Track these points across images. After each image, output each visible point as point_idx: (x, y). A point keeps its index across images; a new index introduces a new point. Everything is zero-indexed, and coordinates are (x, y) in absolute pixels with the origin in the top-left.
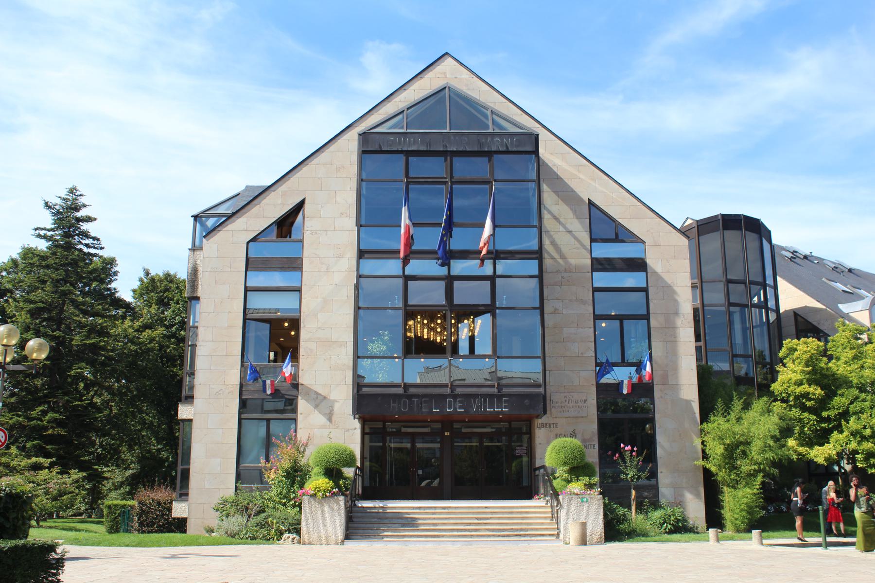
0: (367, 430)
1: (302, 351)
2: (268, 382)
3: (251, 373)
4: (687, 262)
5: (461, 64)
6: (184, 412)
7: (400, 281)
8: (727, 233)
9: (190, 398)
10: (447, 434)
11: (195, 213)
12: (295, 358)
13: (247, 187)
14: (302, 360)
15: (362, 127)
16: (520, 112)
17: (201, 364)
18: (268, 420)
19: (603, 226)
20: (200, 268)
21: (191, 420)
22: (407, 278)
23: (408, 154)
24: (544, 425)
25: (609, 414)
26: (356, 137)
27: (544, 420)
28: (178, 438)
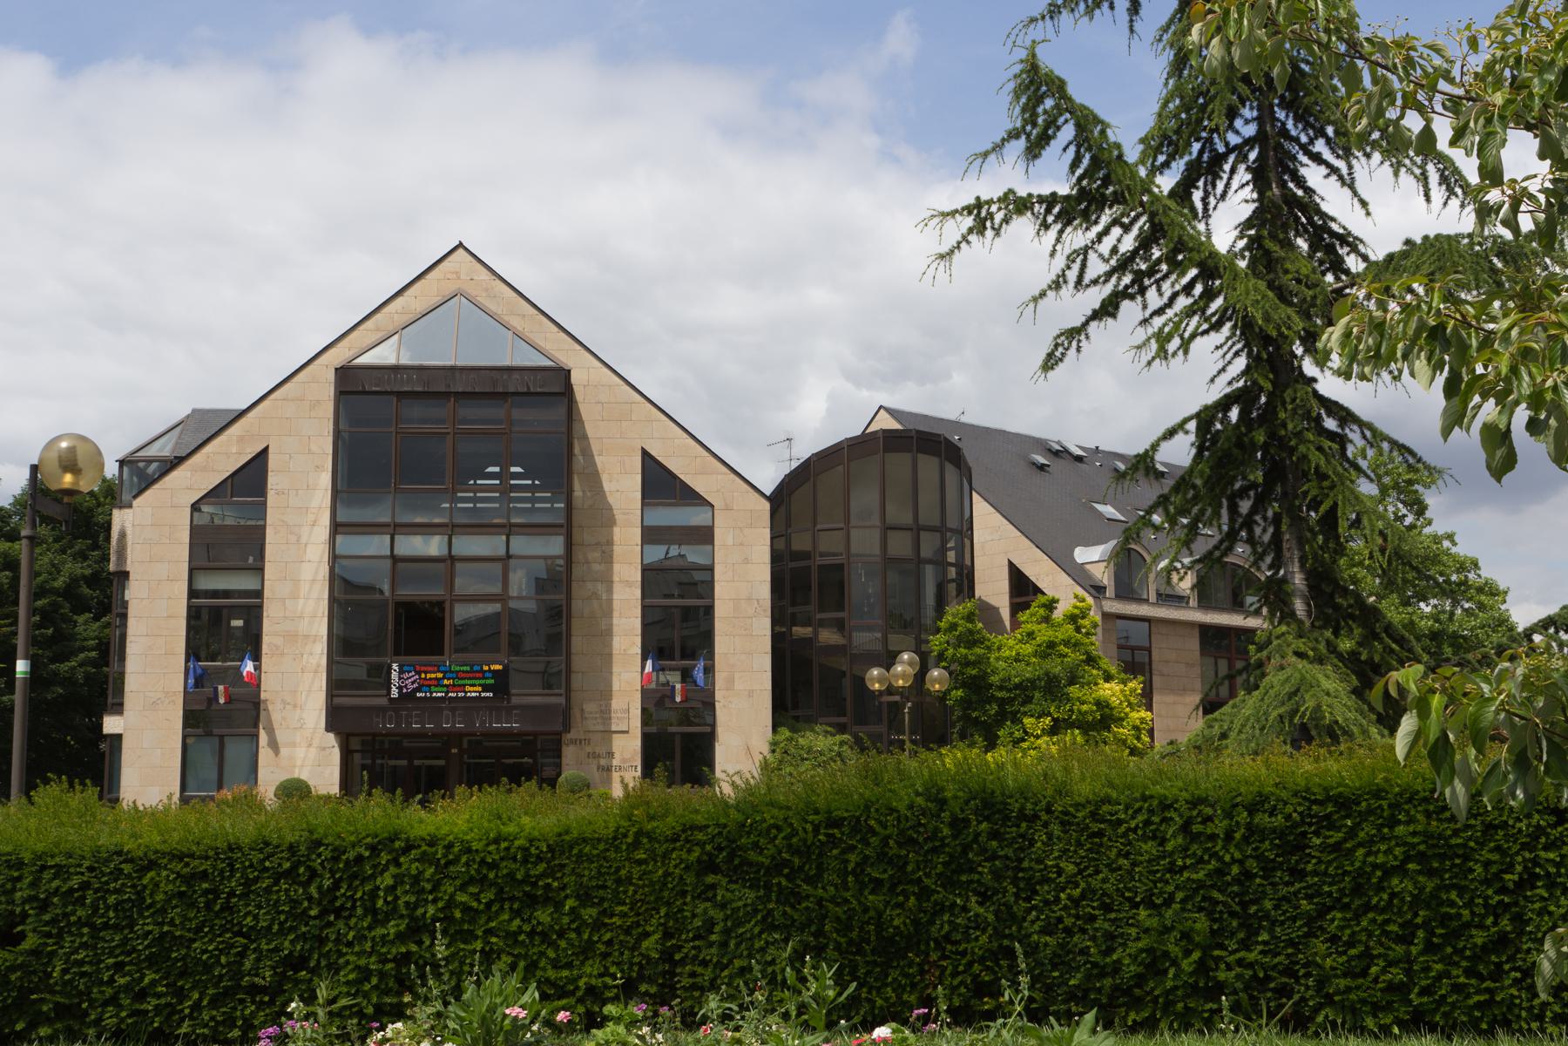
0: (355, 744)
1: (265, 648)
2: (221, 688)
3: (198, 683)
4: (768, 531)
5: (479, 261)
6: (111, 725)
7: (389, 563)
8: (892, 458)
9: (118, 709)
10: (454, 751)
11: (120, 456)
12: (257, 657)
13: (194, 411)
14: (264, 659)
15: (338, 357)
16: (556, 329)
17: (132, 665)
18: (222, 737)
19: (660, 483)
20: (129, 532)
21: (119, 737)
22: (395, 559)
23: (400, 395)
24: (574, 742)
25: (653, 729)
26: (331, 376)
27: (569, 736)
28: (103, 754)
